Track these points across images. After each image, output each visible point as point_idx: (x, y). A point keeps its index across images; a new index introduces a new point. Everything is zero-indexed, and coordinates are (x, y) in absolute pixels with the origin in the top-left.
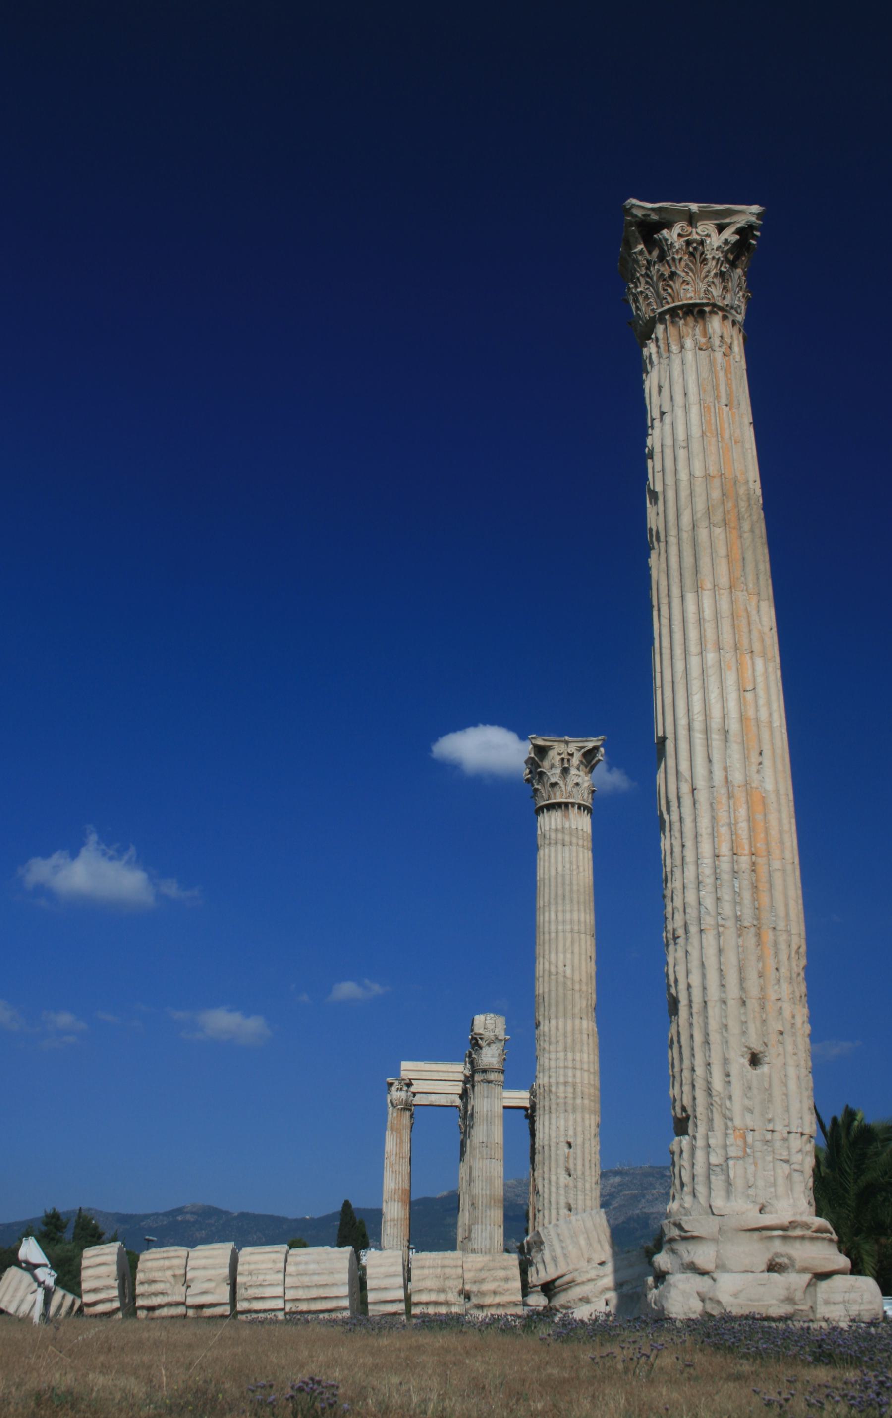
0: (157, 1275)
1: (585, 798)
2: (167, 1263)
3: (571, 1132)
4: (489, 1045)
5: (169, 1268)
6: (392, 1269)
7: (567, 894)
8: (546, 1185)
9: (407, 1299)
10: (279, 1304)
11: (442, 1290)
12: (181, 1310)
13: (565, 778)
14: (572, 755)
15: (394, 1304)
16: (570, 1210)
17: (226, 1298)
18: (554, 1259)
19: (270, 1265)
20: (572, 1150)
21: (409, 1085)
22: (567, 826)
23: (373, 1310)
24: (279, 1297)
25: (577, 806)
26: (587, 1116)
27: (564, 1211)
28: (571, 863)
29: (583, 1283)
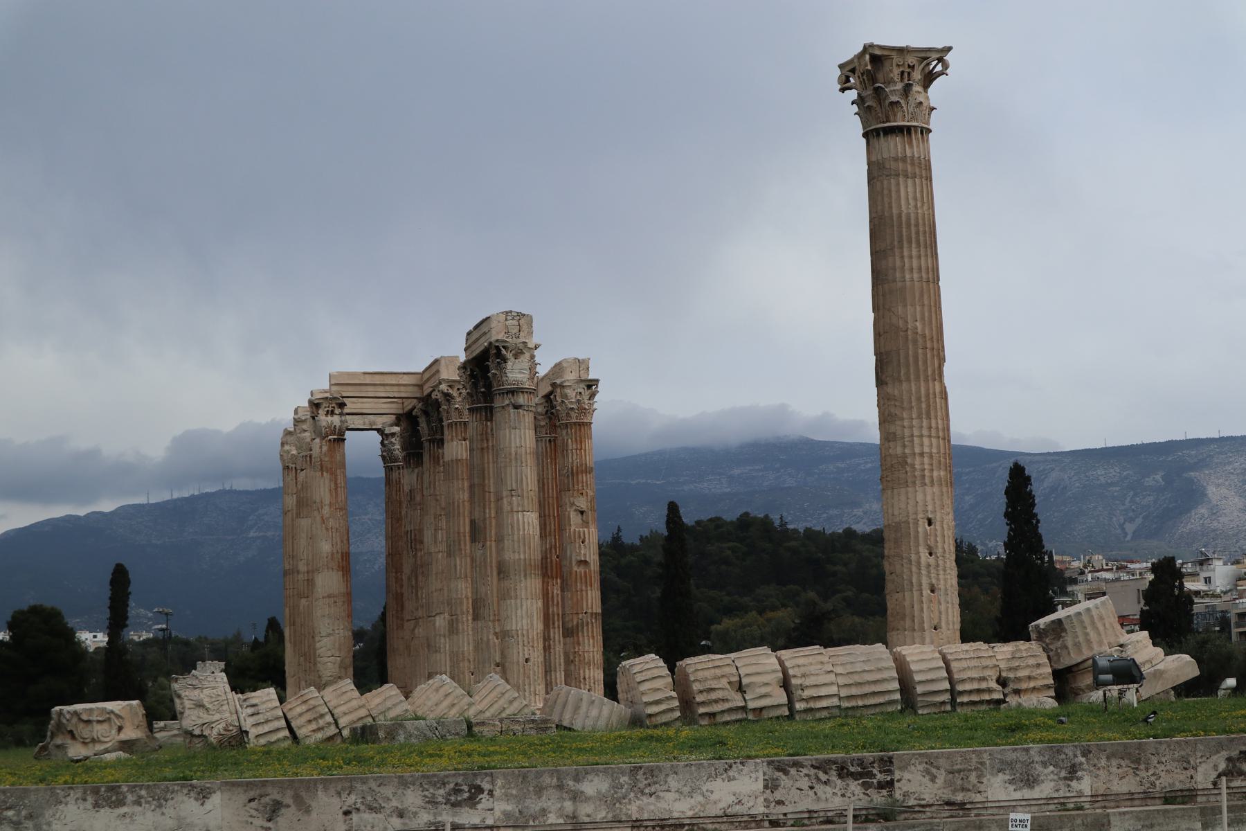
0: (714, 684)
2: (718, 672)
3: (930, 508)
4: (516, 356)
7: (913, 236)
9: (953, 692)
10: (835, 701)
11: (983, 679)
12: (739, 716)
13: (907, 97)
14: (912, 67)
16: (933, 591)
17: (784, 700)
18: (1077, 645)
20: (932, 527)
21: (342, 405)
22: (909, 154)
27: (926, 592)
28: (915, 199)
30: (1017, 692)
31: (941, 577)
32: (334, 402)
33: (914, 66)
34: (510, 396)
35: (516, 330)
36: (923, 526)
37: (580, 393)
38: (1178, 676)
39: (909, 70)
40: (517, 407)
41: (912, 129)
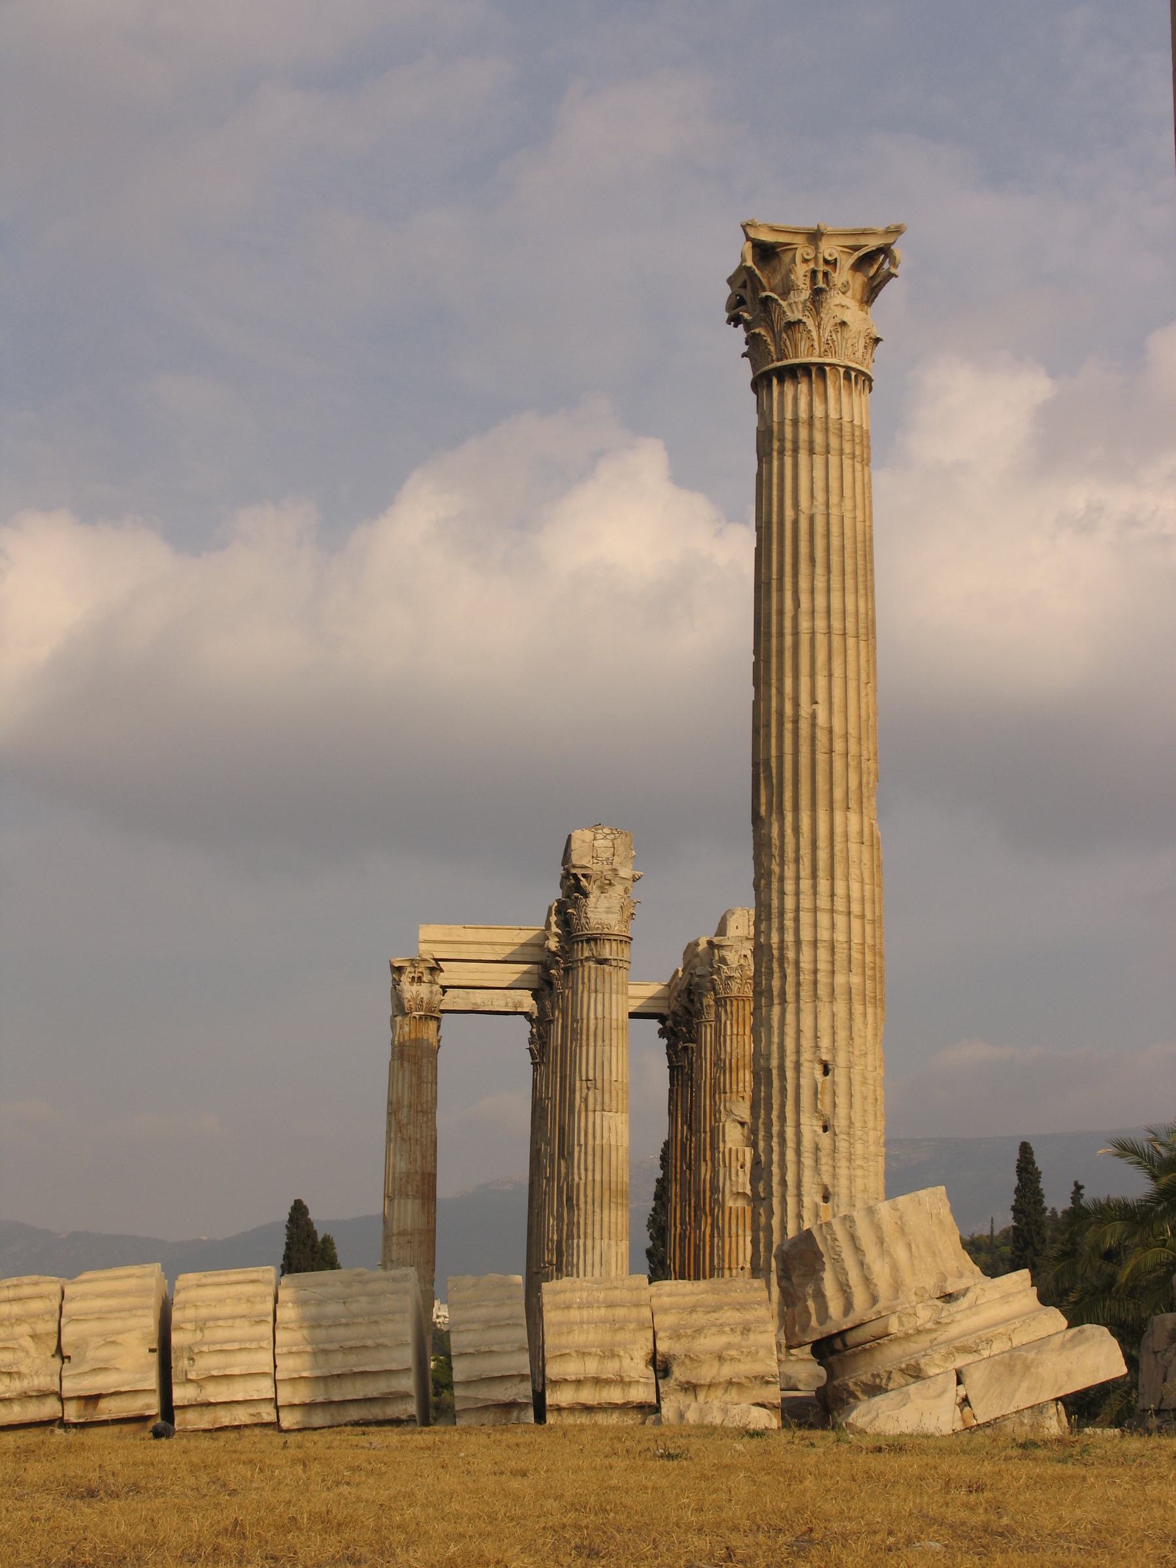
1: (859, 354)
2: (16, 1309)
3: (825, 1042)
5: (19, 1320)
6: (505, 1311)
8: (776, 1147)
12: (50, 1409)
13: (818, 313)
14: (833, 264)
15: (508, 1384)
19: (243, 1308)
20: (828, 1077)
21: (435, 970)
23: (466, 1398)
24: (264, 1374)
25: (842, 370)
26: (858, 1008)
29: (907, 1337)
30: (690, 1388)
31: (843, 1172)
32: (422, 965)
33: (836, 259)
34: (592, 943)
35: (608, 854)
36: (811, 1072)
37: (745, 956)
38: (1069, 1374)
39: (827, 268)
40: (602, 962)
41: (827, 369)
